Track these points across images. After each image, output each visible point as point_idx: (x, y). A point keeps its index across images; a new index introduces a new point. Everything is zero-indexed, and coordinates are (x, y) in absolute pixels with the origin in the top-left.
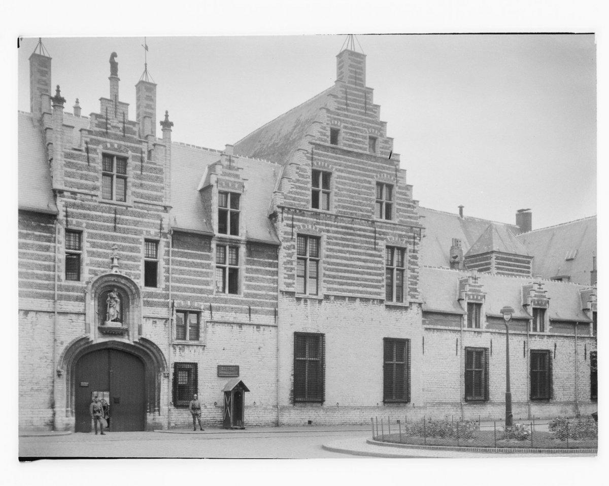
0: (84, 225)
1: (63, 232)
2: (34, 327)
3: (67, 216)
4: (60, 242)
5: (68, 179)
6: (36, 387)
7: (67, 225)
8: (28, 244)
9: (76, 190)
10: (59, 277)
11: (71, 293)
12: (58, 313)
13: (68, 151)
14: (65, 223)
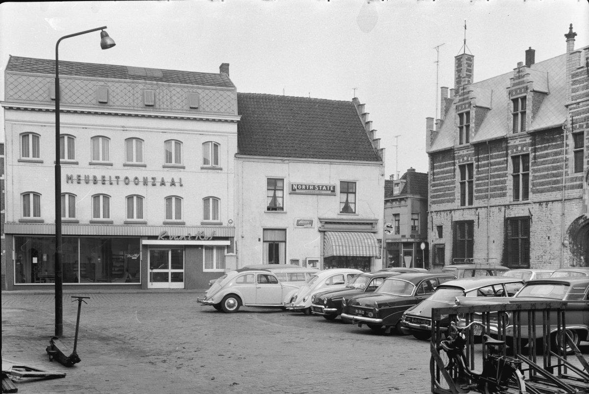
0: (585, 126)
1: (571, 137)
2: (551, 213)
3: (572, 124)
4: (567, 145)
5: (574, 94)
6: (552, 257)
7: (573, 131)
8: (549, 153)
9: (578, 101)
10: (566, 172)
11: (575, 183)
12: (565, 200)
13: (574, 72)
14: (571, 129)
